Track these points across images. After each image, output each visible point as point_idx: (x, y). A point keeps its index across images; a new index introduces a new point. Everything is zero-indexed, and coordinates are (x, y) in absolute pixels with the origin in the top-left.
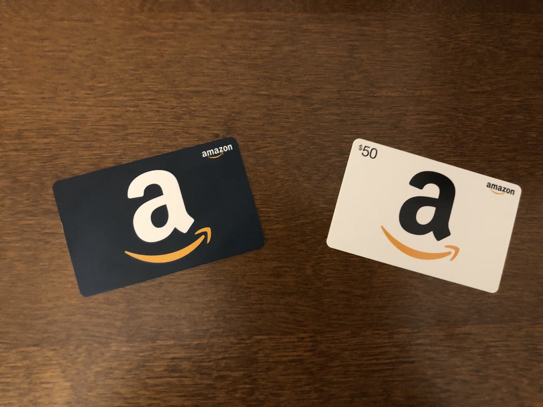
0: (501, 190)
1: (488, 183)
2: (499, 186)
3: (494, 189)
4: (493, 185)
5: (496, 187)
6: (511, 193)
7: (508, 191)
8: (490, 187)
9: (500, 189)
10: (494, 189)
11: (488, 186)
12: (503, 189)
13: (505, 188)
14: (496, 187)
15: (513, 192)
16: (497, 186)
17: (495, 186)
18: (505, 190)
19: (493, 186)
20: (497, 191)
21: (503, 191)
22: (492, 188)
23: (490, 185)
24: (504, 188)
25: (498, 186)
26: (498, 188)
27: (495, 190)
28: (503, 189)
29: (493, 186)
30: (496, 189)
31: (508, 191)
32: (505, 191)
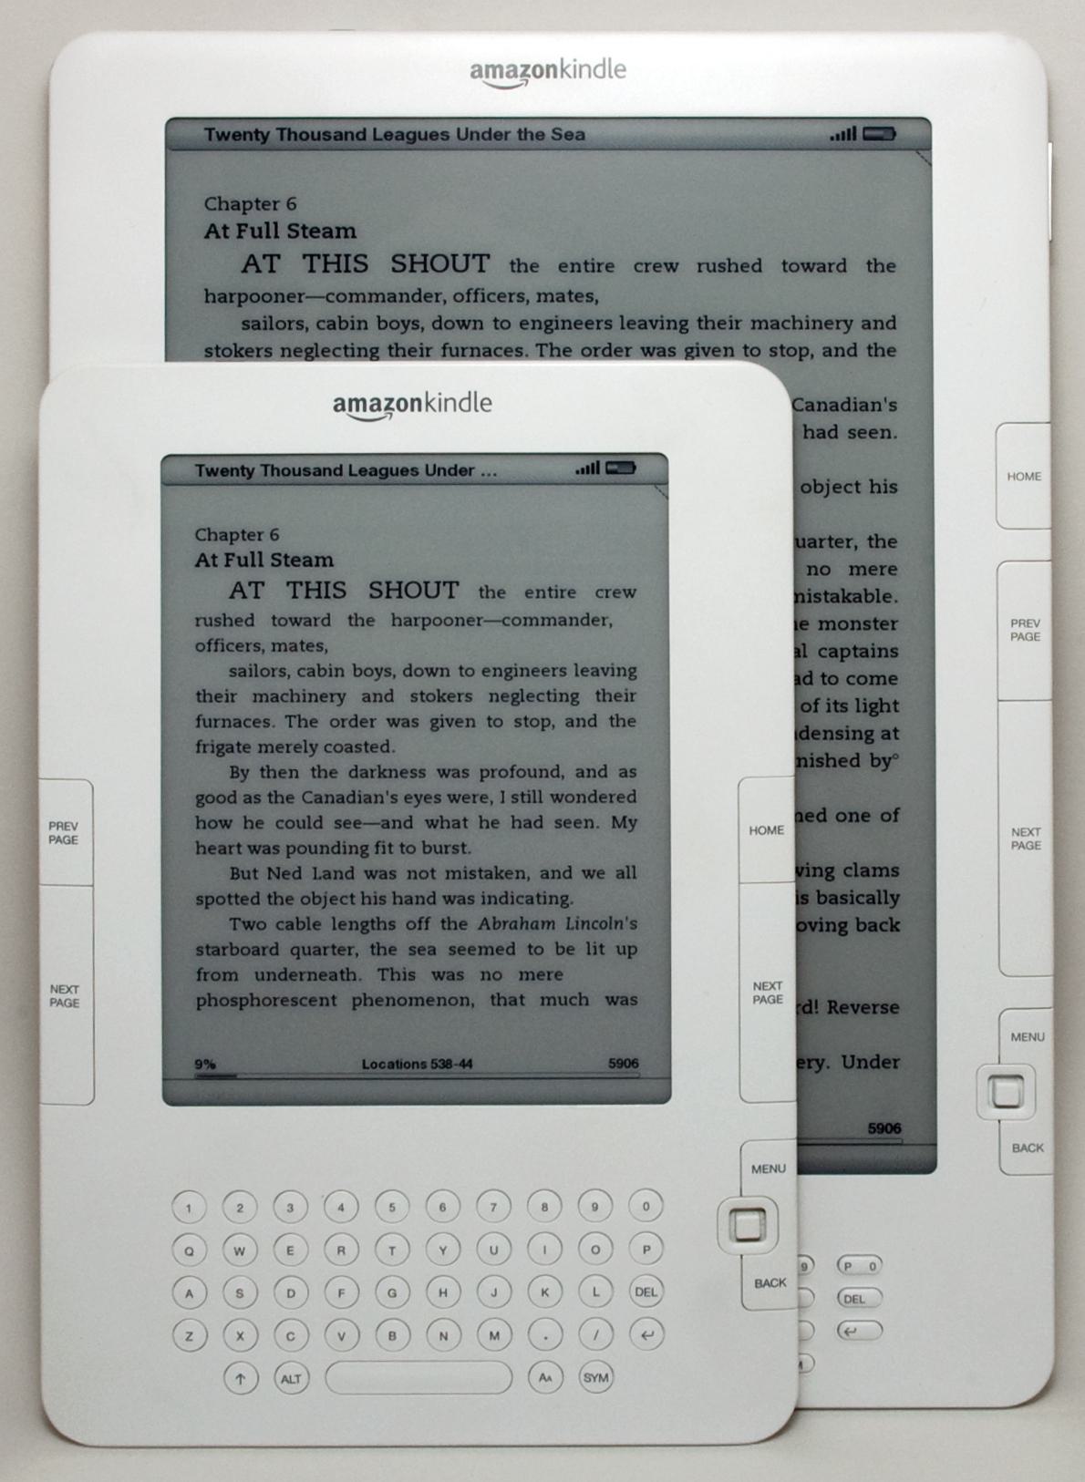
0: (379, 409)
1: (336, 400)
2: (372, 400)
3: (358, 410)
4: (351, 401)
5: (361, 403)
6: (412, 410)
7: (402, 404)
8: (343, 409)
9: (375, 407)
10: (358, 410)
11: (339, 407)
12: (384, 403)
14: (361, 403)
15: (416, 403)
17: (356, 399)
18: (393, 405)
19: (354, 403)
20: (369, 414)
21: (387, 408)
22: (350, 410)
23: (343, 404)
24: (386, 399)
26: (369, 404)
27: (361, 414)
29: (354, 403)
30: (365, 410)
31: (402, 404)
32: (393, 409)
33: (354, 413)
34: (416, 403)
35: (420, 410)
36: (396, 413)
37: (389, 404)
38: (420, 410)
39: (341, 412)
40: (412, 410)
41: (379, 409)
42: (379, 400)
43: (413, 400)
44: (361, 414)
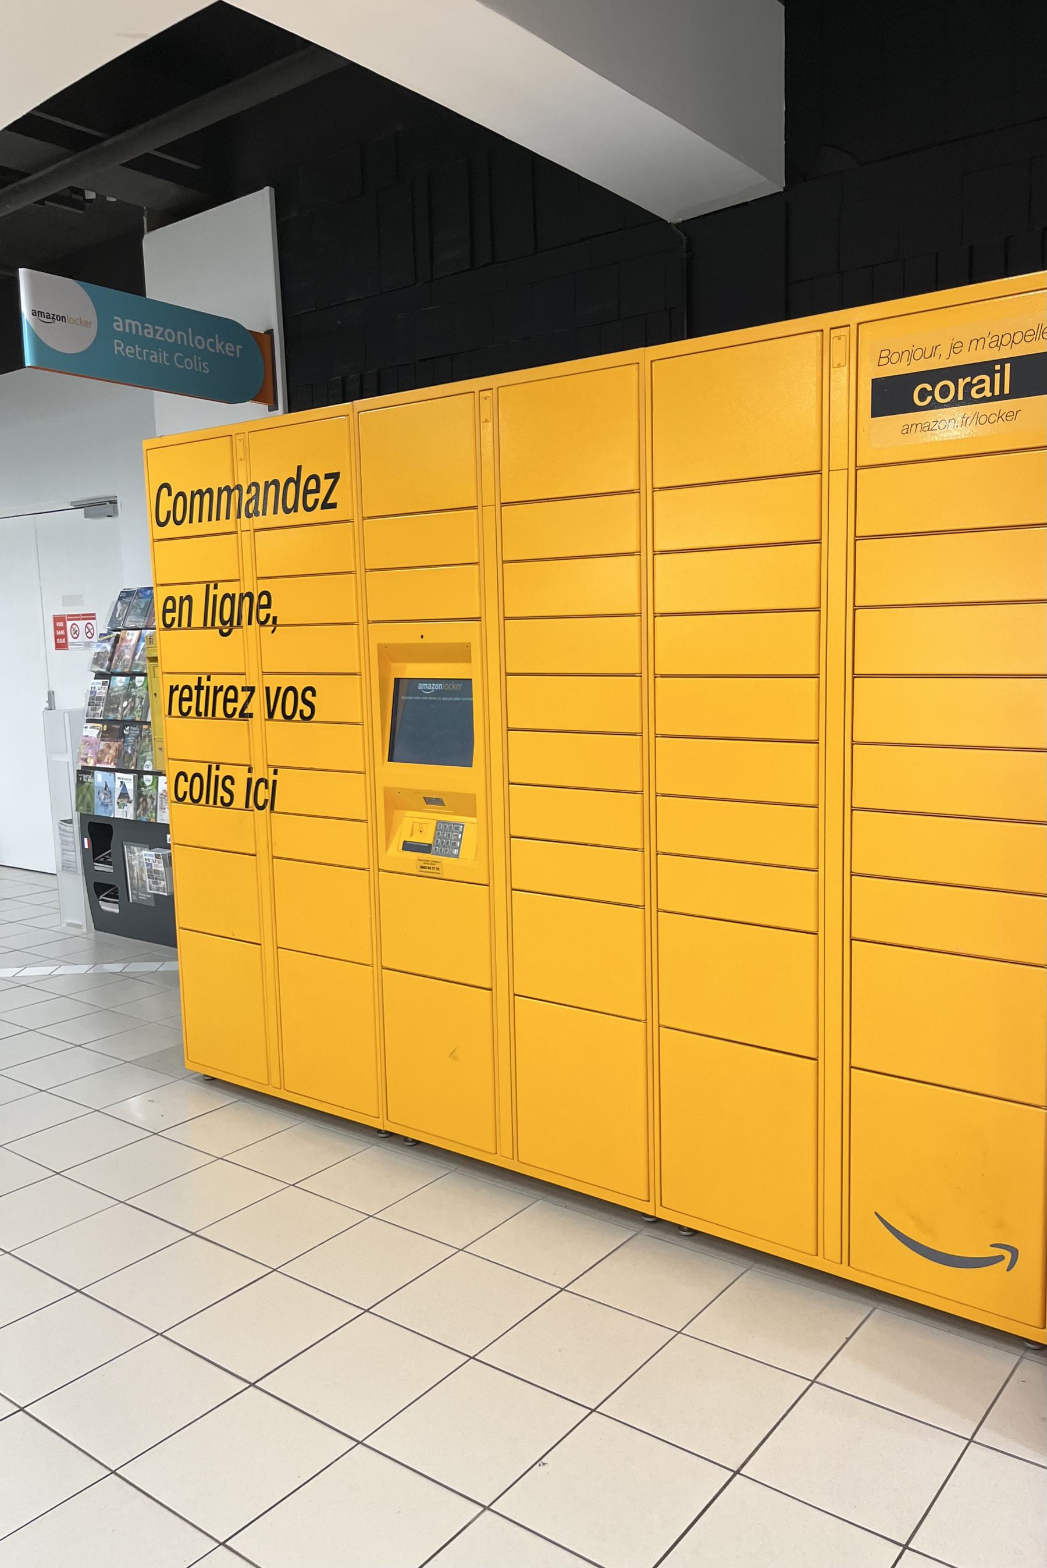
0: (50, 318)
3: (41, 316)
4: (38, 312)
6: (62, 321)
8: (36, 315)
10: (41, 316)
12: (51, 316)
13: (54, 315)
14: (43, 314)
15: (64, 318)
17: (41, 313)
18: (55, 317)
21: (53, 318)
23: (36, 313)
27: (43, 319)
28: (51, 316)
33: (40, 318)
34: (64, 318)
36: (56, 321)
41: (50, 318)
43: (62, 317)
44: (43, 319)
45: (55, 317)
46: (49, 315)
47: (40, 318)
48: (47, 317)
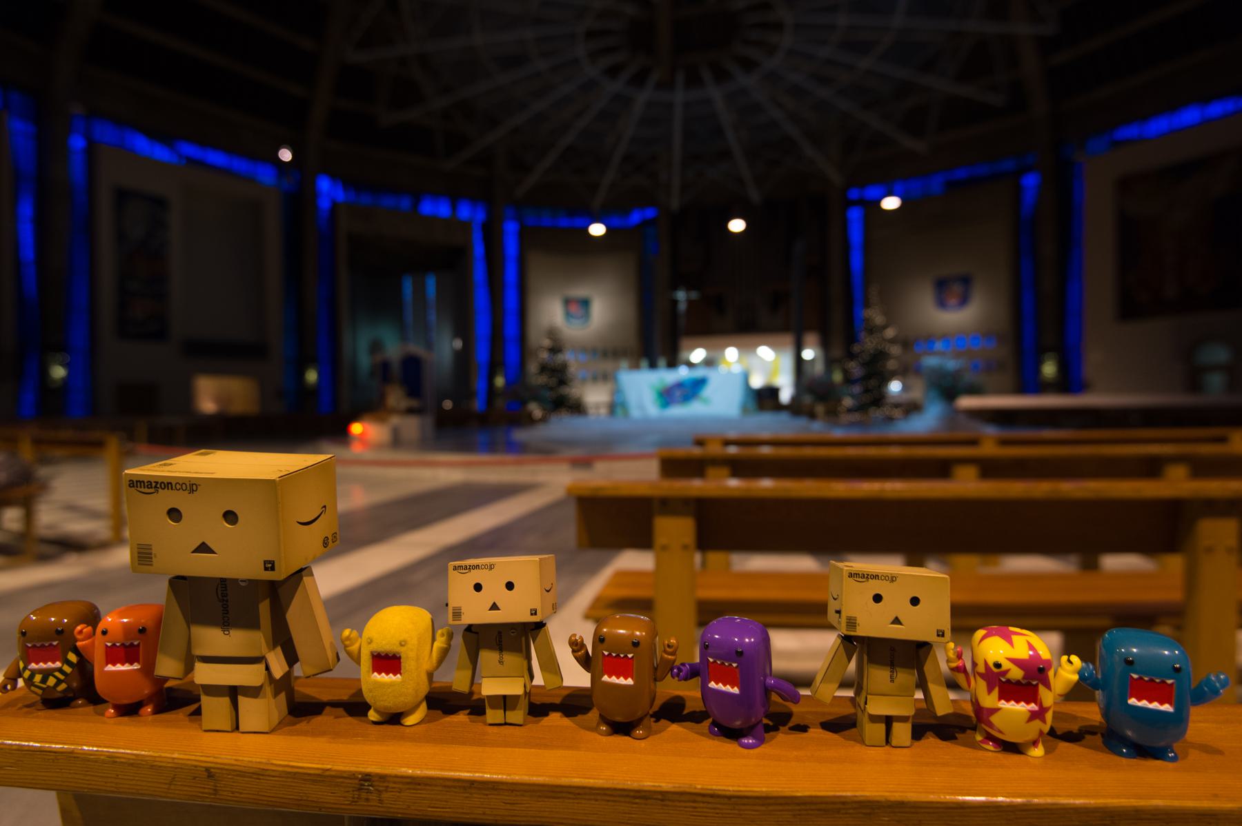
0: (151, 488)
1: (130, 481)
3: (141, 487)
4: (137, 482)
5: (142, 484)
6: (168, 489)
7: (163, 485)
8: (133, 486)
10: (141, 487)
11: (132, 485)
12: (154, 484)
13: (157, 483)
14: (142, 484)
15: (170, 485)
16: (143, 482)
17: (140, 482)
18: (158, 486)
19: (139, 484)
20: (147, 490)
21: (156, 487)
22: (137, 487)
23: (133, 483)
24: (155, 482)
25: (146, 481)
26: (146, 484)
27: (142, 490)
28: (154, 484)
29: (139, 484)
30: (144, 487)
31: (163, 485)
34: (170, 485)
35: (172, 489)
36: (160, 490)
37: (156, 485)
38: (172, 489)
39: (133, 489)
40: (168, 489)
42: (151, 482)
43: (168, 483)
45: (158, 486)
46: (151, 484)
47: (139, 489)
48: (149, 488)
